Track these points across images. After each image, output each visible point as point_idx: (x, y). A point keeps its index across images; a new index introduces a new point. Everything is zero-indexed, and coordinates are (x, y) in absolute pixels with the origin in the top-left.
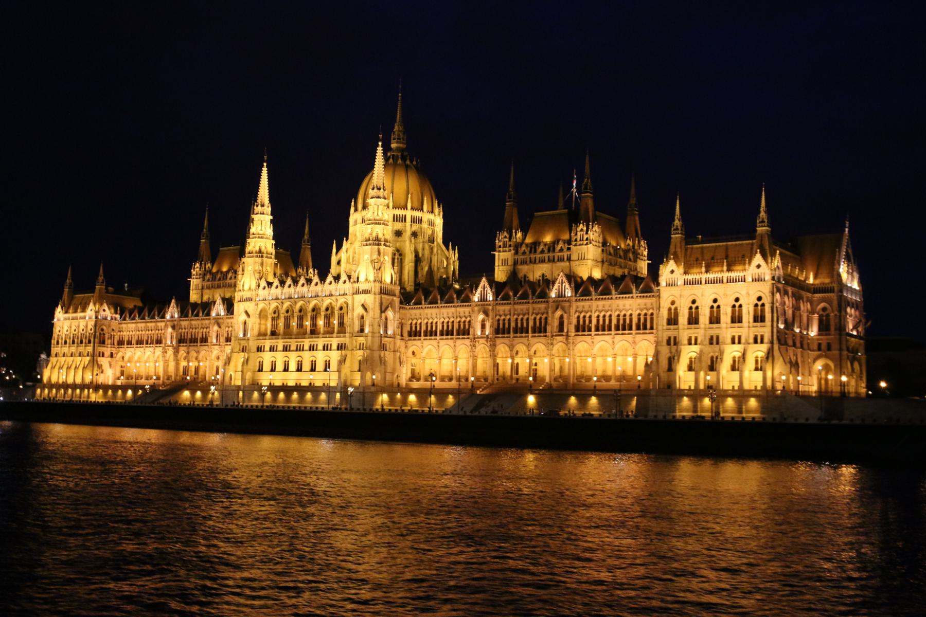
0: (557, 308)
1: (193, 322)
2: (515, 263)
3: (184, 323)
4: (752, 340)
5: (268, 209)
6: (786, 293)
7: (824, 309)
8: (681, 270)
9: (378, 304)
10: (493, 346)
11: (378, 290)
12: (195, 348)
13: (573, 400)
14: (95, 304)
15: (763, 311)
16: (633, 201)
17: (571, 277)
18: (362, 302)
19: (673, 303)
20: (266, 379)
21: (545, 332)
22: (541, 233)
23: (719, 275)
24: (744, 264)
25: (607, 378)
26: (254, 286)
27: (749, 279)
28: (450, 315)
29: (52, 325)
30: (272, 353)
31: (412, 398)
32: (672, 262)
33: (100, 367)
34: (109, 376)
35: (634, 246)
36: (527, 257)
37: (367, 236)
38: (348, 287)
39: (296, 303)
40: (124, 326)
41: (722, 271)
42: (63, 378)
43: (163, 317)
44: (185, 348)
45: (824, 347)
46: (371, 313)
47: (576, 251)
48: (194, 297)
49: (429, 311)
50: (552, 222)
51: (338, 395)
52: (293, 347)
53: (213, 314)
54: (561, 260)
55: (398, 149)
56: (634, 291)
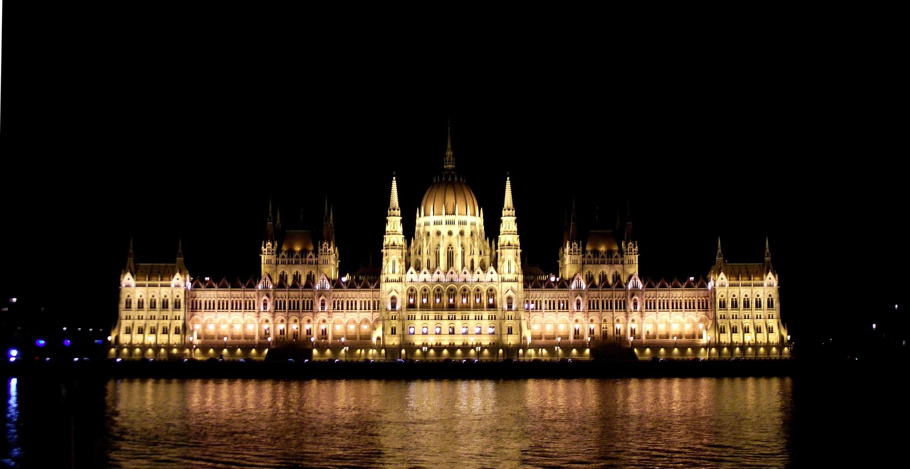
0: (633, 296)
1: (292, 293)
2: (583, 263)
5: (398, 212)
12: (297, 314)
14: (180, 273)
18: (509, 287)
20: (418, 341)
22: (596, 244)
23: (748, 282)
30: (424, 321)
31: (544, 351)
38: (495, 276)
47: (627, 258)
48: (265, 269)
50: (604, 238)
51: (501, 351)
53: (317, 287)
54: (617, 263)
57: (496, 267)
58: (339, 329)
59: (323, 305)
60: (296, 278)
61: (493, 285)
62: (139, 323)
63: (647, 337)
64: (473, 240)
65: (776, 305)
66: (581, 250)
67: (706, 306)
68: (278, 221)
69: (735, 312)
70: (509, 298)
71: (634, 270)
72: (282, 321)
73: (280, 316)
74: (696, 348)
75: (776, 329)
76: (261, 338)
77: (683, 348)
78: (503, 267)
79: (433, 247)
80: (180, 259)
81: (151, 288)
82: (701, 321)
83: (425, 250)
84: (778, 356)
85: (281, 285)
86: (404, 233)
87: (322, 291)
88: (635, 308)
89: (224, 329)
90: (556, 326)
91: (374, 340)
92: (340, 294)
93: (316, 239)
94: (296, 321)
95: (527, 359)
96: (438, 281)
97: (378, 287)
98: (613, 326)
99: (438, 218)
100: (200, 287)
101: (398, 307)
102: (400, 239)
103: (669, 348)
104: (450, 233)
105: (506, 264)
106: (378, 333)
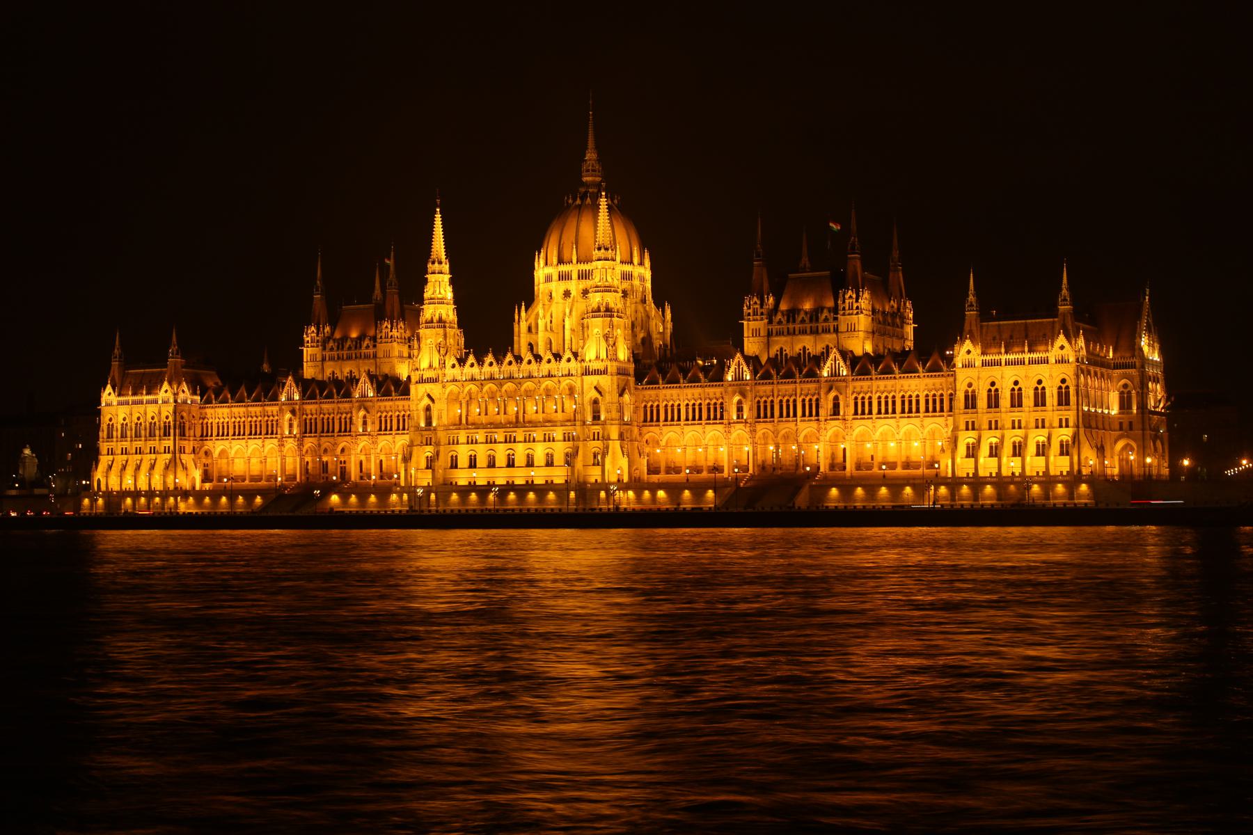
0: (830, 389)
1: (324, 406)
2: (769, 334)
3: (310, 407)
4: (1056, 424)
5: (446, 267)
6: (1089, 373)
7: (1125, 386)
8: (979, 351)
9: (615, 386)
10: (753, 431)
11: (615, 370)
12: (331, 440)
14: (170, 384)
15: (1067, 394)
16: (896, 254)
17: (844, 354)
18: (595, 384)
19: (970, 385)
20: (462, 477)
21: (817, 415)
23: (1020, 356)
24: (1047, 344)
25: (892, 466)
26: (436, 364)
27: (1052, 360)
28: (696, 396)
29: (99, 413)
31: (661, 494)
32: (968, 342)
33: (185, 468)
34: (192, 477)
35: (899, 309)
36: (784, 327)
37: (595, 306)
38: (574, 365)
39: (501, 385)
40: (209, 411)
41: (1023, 352)
42: (128, 483)
43: (275, 398)
44: (314, 440)
45: (1125, 426)
46: (608, 397)
48: (309, 371)
49: (668, 392)
51: (572, 494)
54: (826, 331)
56: (920, 369)
59: (365, 423)
63: (858, 467)
69: (992, 416)
70: (596, 402)
73: (309, 442)
77: (895, 486)
80: (174, 360)
84: (888, 504)
86: (457, 300)
87: (363, 403)
88: (836, 410)
92: (388, 404)
93: (380, 315)
96: (492, 378)
99: (549, 270)
100: (211, 402)
102: (448, 312)
103: (871, 486)
104: (567, 294)
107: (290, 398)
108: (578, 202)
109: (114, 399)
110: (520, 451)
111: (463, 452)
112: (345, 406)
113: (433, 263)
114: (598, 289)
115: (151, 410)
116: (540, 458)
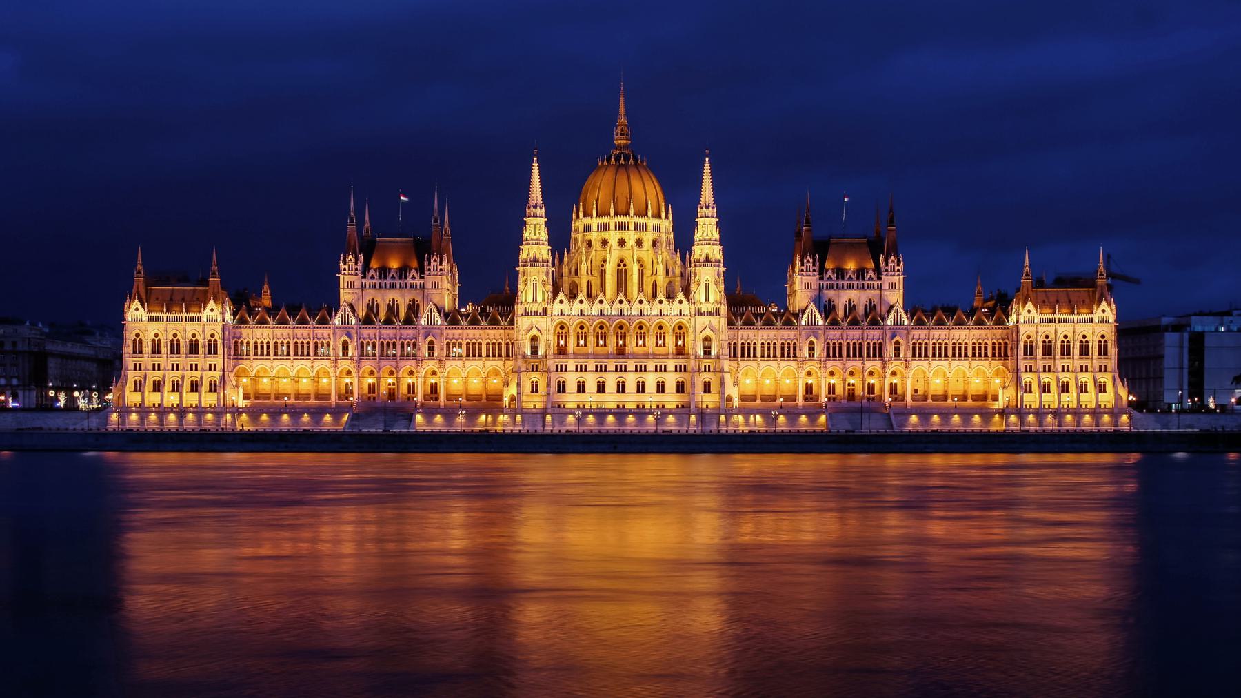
0: (893, 336)
1: (385, 332)
2: (821, 288)
12: (393, 363)
13: (936, 418)
14: (215, 300)
15: (1106, 346)
20: (571, 400)
22: (840, 258)
30: (579, 374)
31: (758, 417)
38: (685, 305)
47: (886, 280)
48: (345, 295)
51: (693, 418)
52: (611, 367)
54: (871, 287)
55: (626, 147)
57: (687, 291)
58: (456, 384)
59: (431, 348)
60: (392, 309)
61: (683, 320)
62: (154, 376)
64: (656, 253)
65: (1113, 350)
66: (817, 269)
67: (1003, 352)
68: (367, 225)
69: (1047, 362)
70: (707, 339)
71: (896, 297)
72: (372, 373)
73: (367, 365)
74: (987, 415)
75: (1109, 388)
76: (340, 397)
77: (966, 414)
78: (699, 294)
79: (597, 263)
80: (214, 281)
81: (171, 325)
82: (997, 373)
83: (584, 268)
85: (367, 321)
87: (430, 328)
88: (897, 354)
89: (285, 385)
90: (777, 381)
91: (506, 400)
92: (457, 333)
93: (422, 251)
94: (391, 373)
95: (731, 429)
96: (601, 313)
97: (512, 322)
98: (864, 381)
99: (605, 220)
100: (246, 322)
101: (541, 352)
102: (544, 252)
103: (946, 415)
104: (622, 243)
105: (702, 288)
106: (513, 390)
107: (345, 322)
108: (622, 161)
109: (143, 314)
110: (631, 380)
111: (571, 379)
112: (410, 333)
113: (535, 207)
114: (707, 242)
115: (192, 328)
116: (651, 386)
